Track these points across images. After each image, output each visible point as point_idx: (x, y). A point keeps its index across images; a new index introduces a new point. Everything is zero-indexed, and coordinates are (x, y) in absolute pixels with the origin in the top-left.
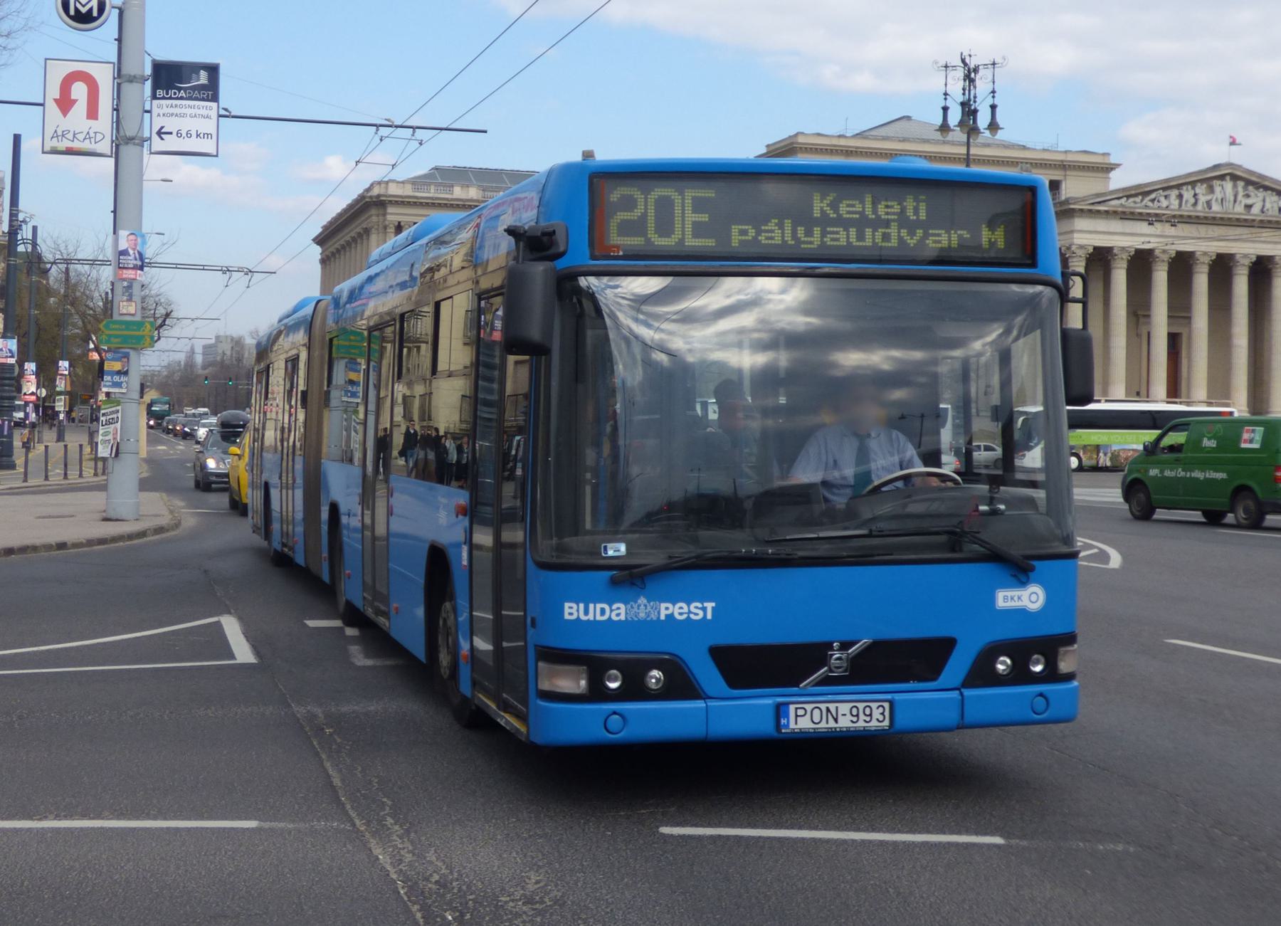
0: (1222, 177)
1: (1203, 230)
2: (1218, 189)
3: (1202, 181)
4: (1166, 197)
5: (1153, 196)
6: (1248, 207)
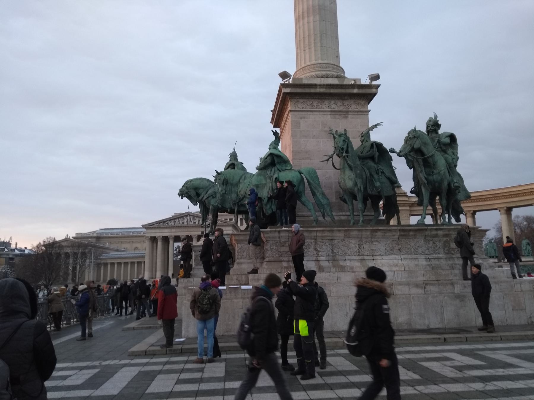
0: (187, 216)
2: (185, 219)
3: (181, 217)
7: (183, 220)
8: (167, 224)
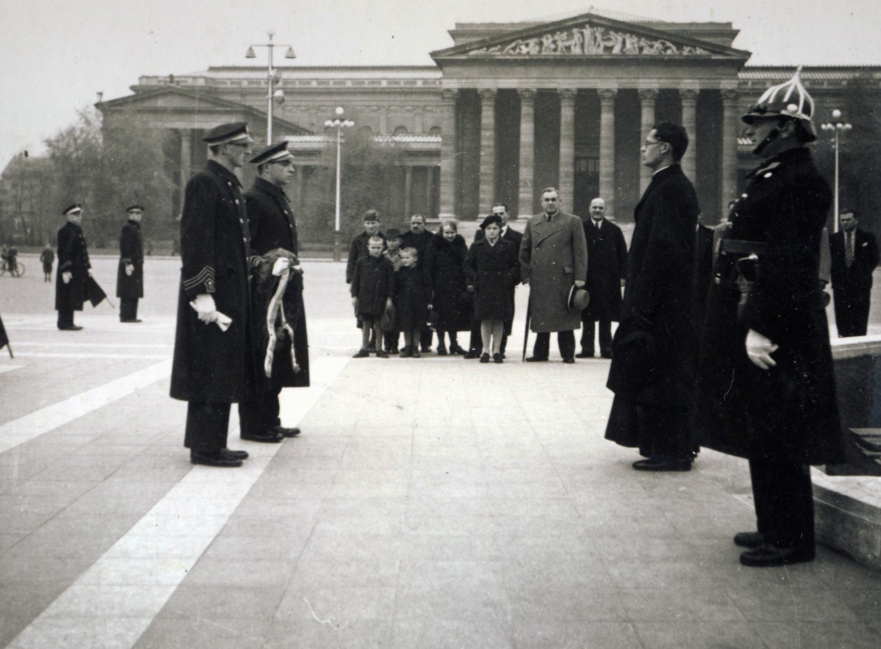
1: (559, 71)
2: (577, 36)
4: (527, 45)
5: (513, 45)
6: (608, 49)
7: (568, 40)
8: (514, 49)
